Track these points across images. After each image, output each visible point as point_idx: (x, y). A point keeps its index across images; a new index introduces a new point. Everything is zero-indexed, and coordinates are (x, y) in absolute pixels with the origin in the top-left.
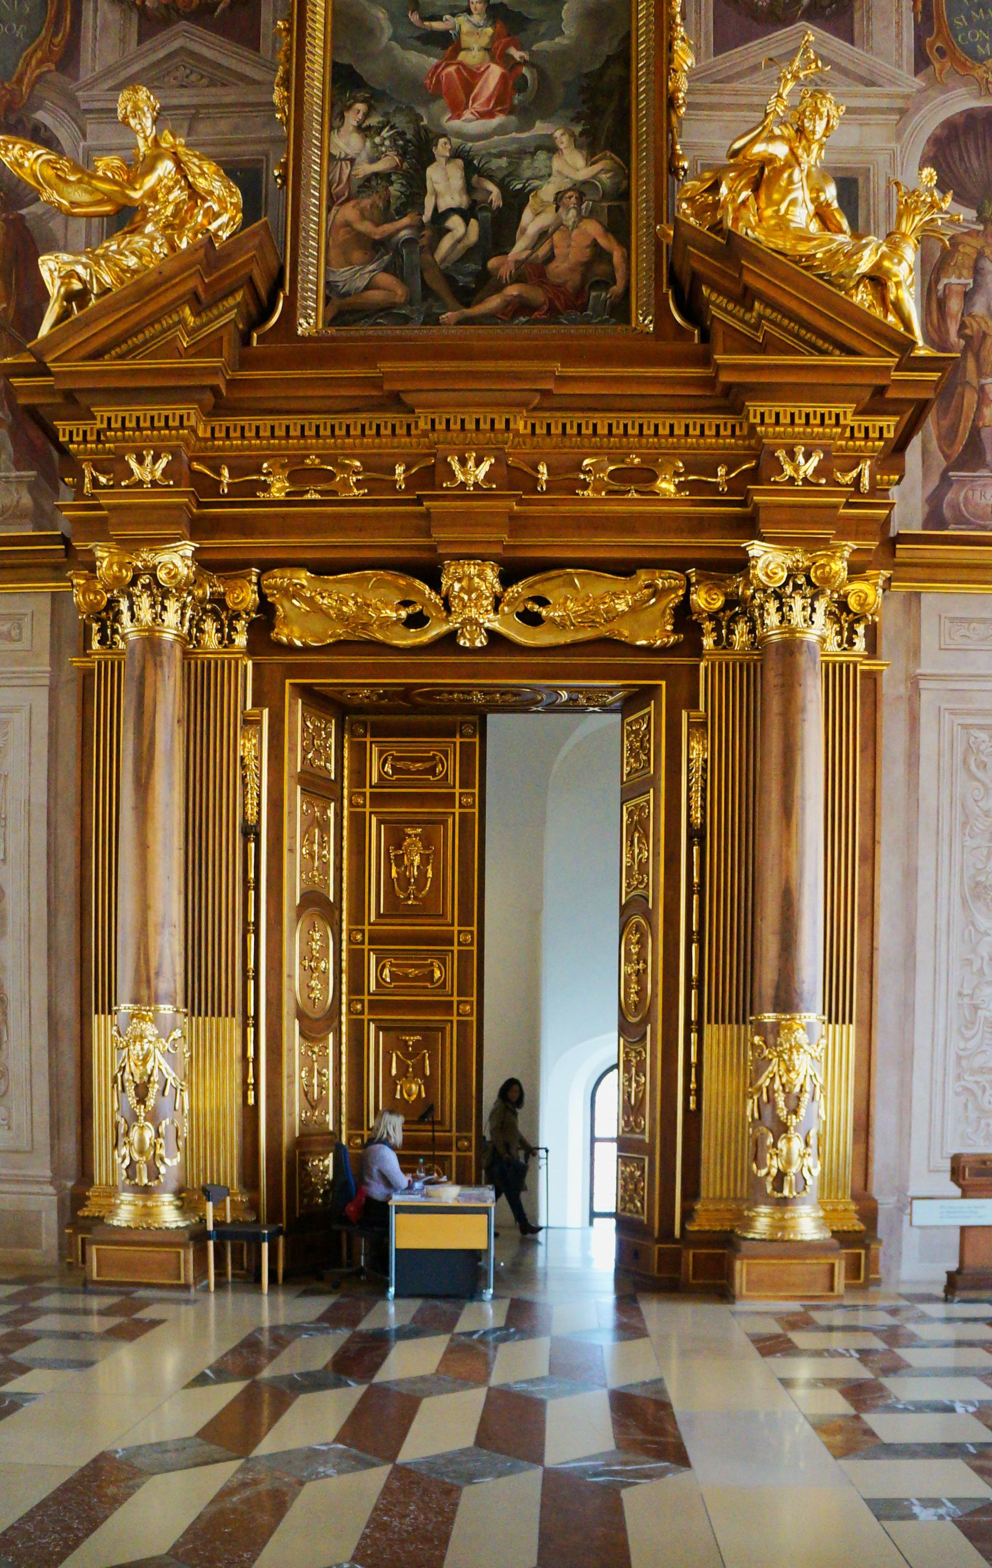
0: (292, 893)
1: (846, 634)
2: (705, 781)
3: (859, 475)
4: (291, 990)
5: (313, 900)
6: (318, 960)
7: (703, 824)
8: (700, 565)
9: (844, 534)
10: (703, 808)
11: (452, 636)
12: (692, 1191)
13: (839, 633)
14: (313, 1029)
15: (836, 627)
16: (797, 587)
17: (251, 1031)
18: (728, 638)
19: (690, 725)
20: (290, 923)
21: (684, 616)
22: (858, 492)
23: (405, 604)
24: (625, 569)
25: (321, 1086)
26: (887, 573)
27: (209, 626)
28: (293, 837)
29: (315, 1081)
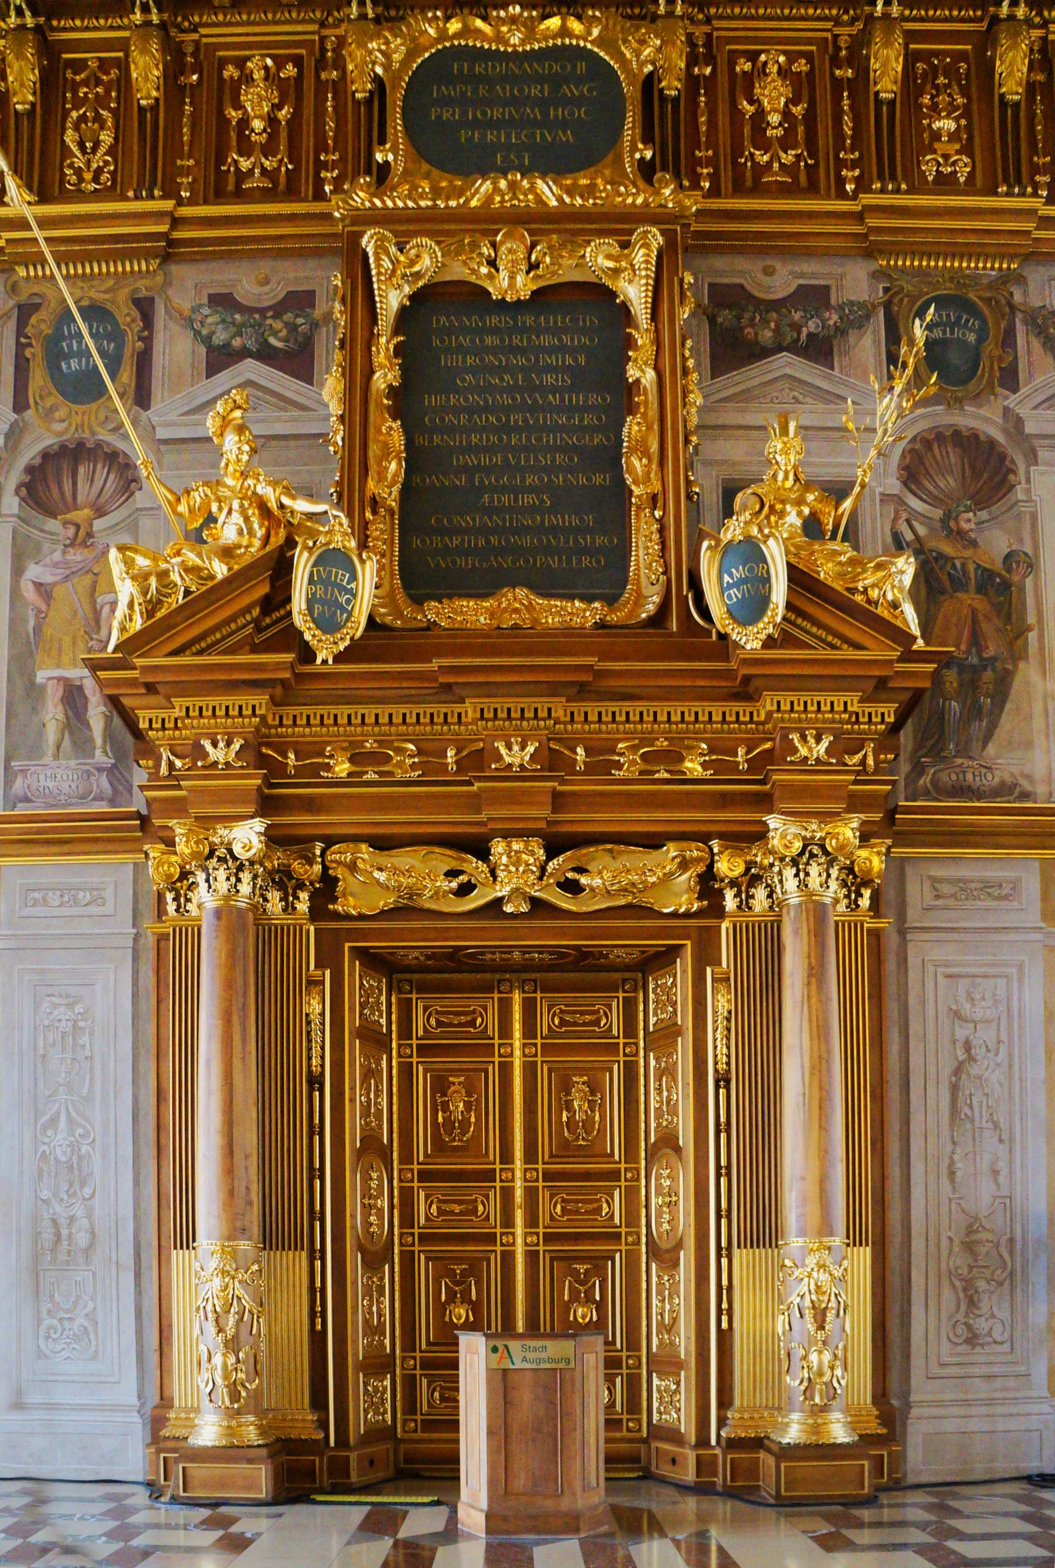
0: (353, 1137)
1: (853, 896)
2: (729, 1029)
3: (865, 755)
4: (354, 1227)
5: (372, 1147)
6: (377, 1198)
7: (729, 1071)
8: (721, 836)
9: (851, 809)
10: (728, 1056)
11: (499, 902)
12: (725, 1402)
13: (847, 896)
14: (374, 1260)
15: (845, 891)
16: (812, 856)
17: (318, 1263)
18: (747, 903)
19: (714, 980)
20: (351, 1164)
21: (708, 885)
22: (865, 771)
23: (452, 874)
24: (653, 842)
25: (380, 1315)
26: (889, 842)
27: (274, 896)
28: (353, 1088)
29: (374, 1309)
